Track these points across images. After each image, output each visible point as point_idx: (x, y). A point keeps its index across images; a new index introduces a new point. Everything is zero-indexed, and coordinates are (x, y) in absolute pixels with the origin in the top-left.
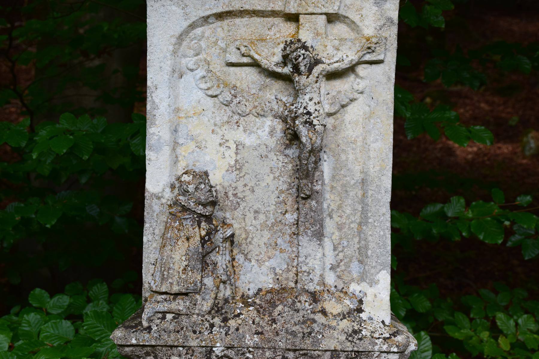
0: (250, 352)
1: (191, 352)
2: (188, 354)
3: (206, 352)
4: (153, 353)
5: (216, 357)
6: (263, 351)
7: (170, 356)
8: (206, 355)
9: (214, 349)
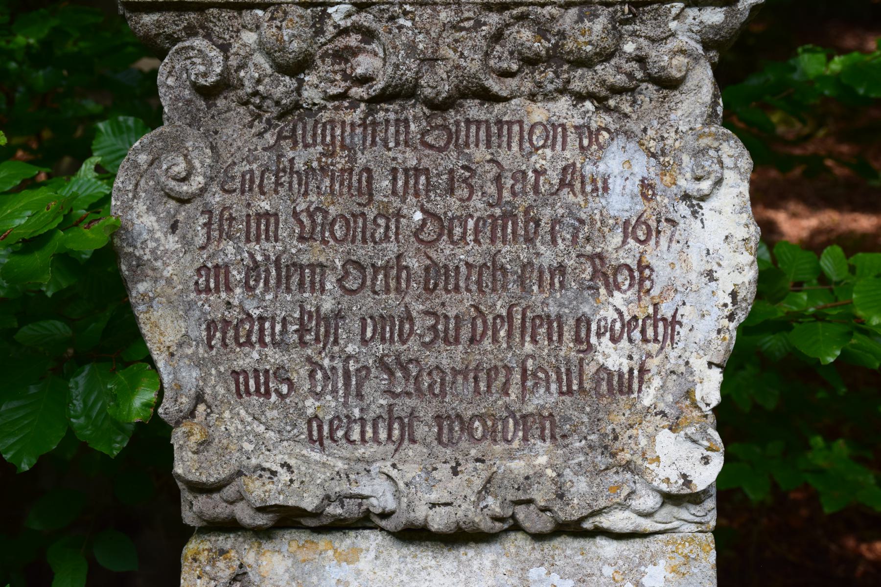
0: (405, 13)
1: (281, 14)
2: (275, 19)
3: (313, 17)
4: (203, 27)
5: (335, 27)
6: (434, 10)
7: (238, 31)
8: (314, 25)
9: (330, 10)
